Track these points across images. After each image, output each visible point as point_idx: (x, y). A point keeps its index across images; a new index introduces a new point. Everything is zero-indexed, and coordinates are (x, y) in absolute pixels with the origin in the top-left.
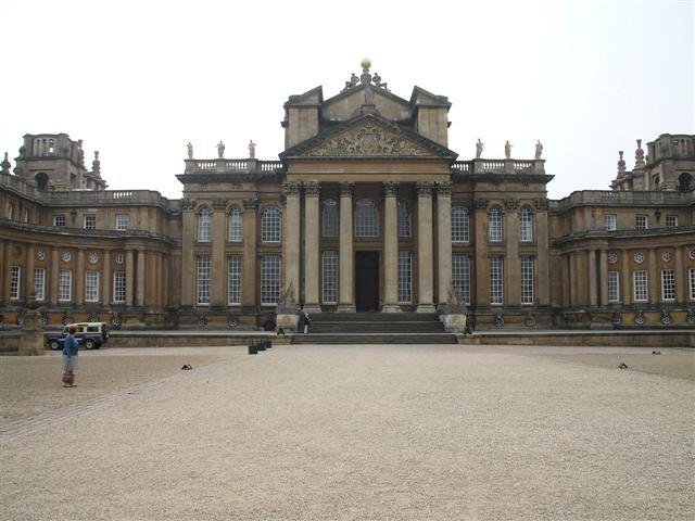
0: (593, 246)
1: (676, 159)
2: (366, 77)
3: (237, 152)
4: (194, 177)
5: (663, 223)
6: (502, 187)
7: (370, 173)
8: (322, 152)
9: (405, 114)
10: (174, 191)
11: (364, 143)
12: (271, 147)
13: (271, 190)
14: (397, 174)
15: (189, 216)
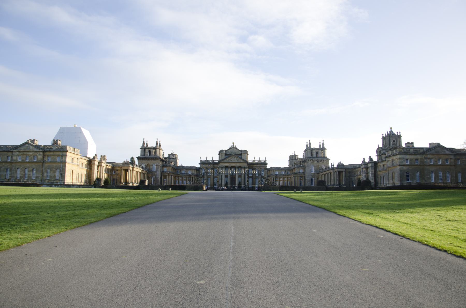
0: (272, 177)
1: (292, 160)
2: (233, 146)
3: (210, 159)
4: (202, 163)
5: (287, 173)
6: (258, 166)
7: (233, 165)
8: (225, 161)
9: (240, 153)
10: (198, 166)
11: (232, 159)
12: (216, 158)
13: (216, 165)
14: (238, 165)
15: (201, 170)
